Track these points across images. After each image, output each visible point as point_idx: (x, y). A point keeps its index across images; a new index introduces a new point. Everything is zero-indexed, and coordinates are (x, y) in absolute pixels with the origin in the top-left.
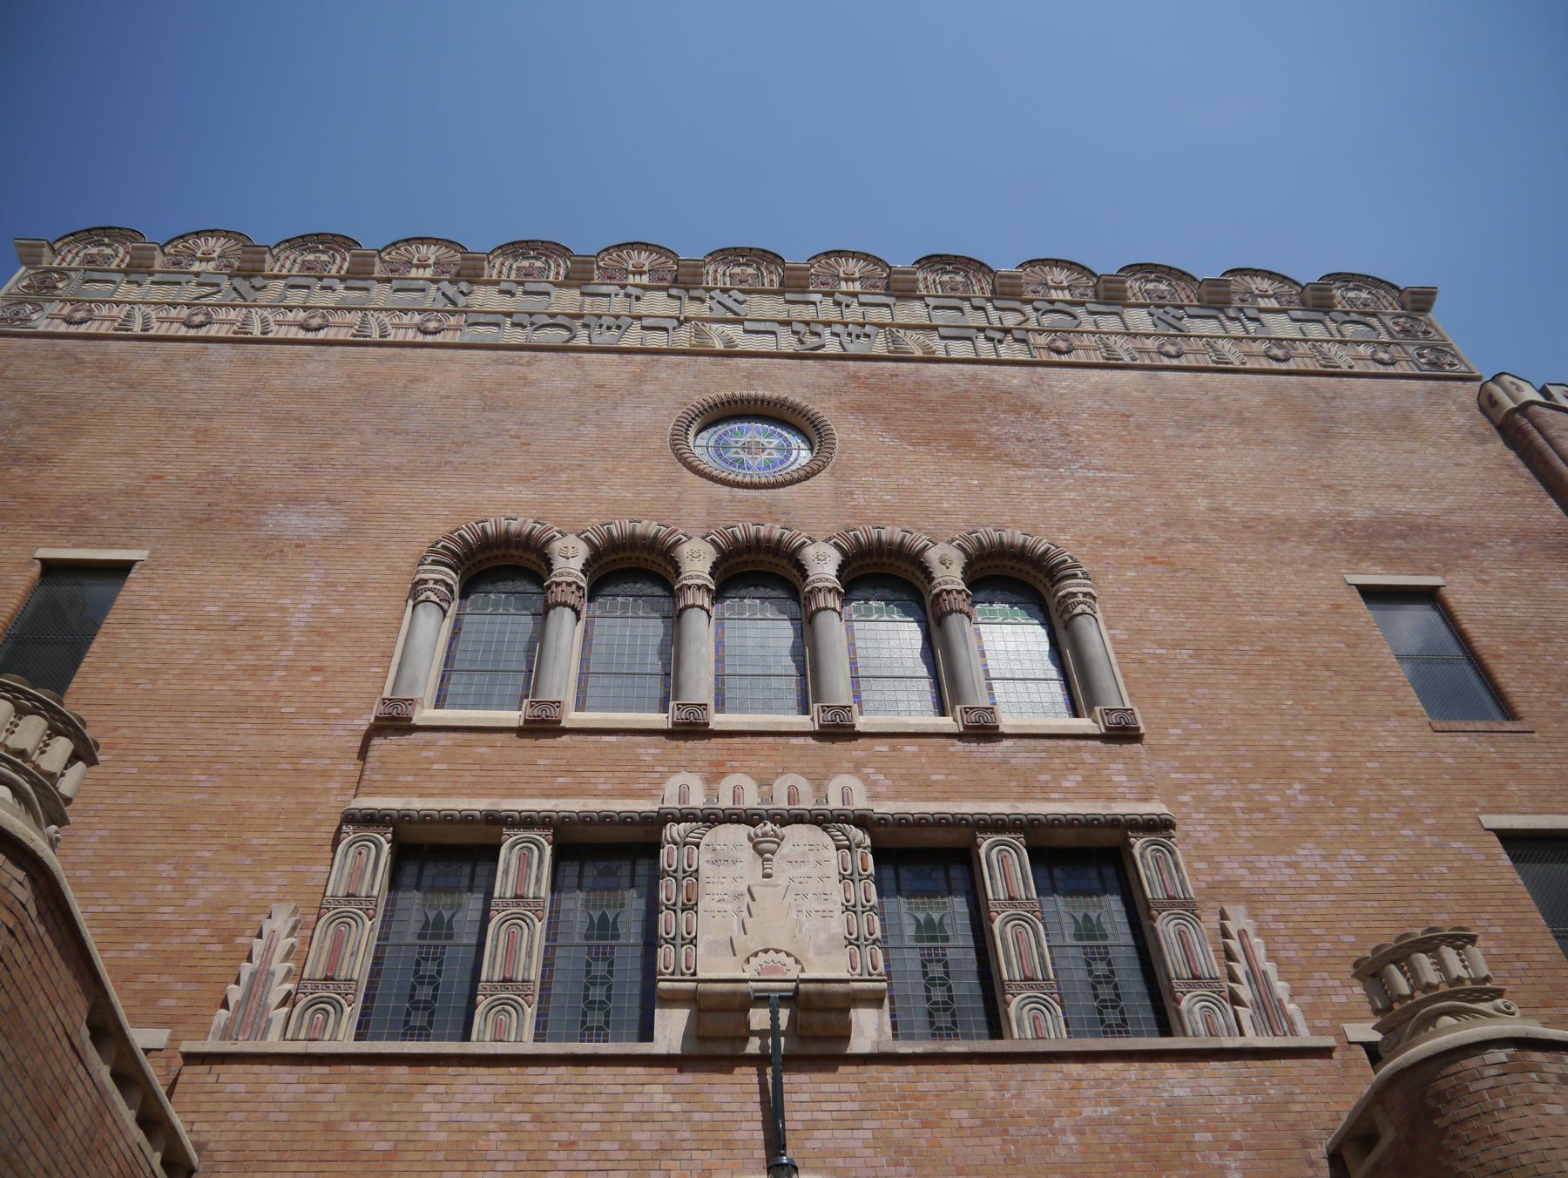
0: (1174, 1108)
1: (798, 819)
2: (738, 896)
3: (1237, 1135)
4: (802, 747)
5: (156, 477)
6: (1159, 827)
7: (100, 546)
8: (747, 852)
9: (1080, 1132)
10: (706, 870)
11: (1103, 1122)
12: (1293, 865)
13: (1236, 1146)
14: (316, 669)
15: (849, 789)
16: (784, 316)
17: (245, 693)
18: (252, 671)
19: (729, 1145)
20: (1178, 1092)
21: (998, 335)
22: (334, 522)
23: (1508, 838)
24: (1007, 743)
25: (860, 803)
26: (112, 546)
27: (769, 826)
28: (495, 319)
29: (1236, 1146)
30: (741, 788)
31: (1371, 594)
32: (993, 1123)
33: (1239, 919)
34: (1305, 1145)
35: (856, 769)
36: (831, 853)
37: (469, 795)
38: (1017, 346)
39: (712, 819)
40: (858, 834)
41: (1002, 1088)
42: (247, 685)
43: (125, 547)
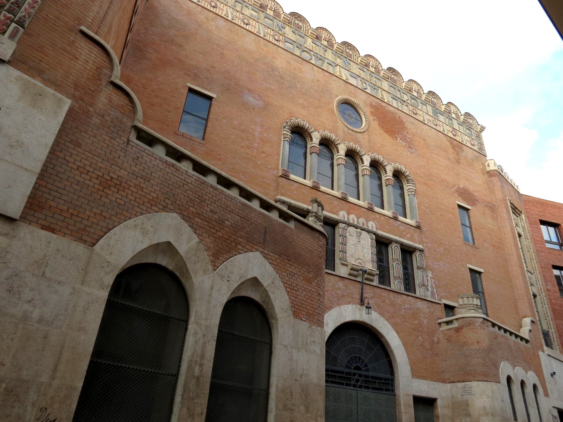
0: (418, 309)
1: (364, 230)
2: (354, 245)
3: (426, 316)
4: (364, 211)
5: (213, 67)
6: (421, 251)
7: (203, 88)
8: (355, 235)
9: (405, 309)
10: (348, 236)
11: (408, 308)
12: (439, 265)
13: (426, 318)
14: (264, 152)
15: (372, 226)
16: (358, 74)
17: (248, 154)
18: (249, 147)
19: (352, 298)
20: (420, 306)
21: (402, 102)
22: (260, 103)
23: (471, 270)
24: (399, 223)
25: (375, 230)
26: (206, 89)
27: (359, 230)
28: (292, 42)
29: (426, 318)
30: (352, 218)
31: (459, 206)
32: (393, 305)
33: (430, 274)
34: (435, 320)
35: (373, 220)
36: (370, 240)
37: (301, 202)
38: (406, 107)
39: (350, 225)
40: (374, 237)
41: (394, 298)
42: (248, 151)
43: (210, 91)
